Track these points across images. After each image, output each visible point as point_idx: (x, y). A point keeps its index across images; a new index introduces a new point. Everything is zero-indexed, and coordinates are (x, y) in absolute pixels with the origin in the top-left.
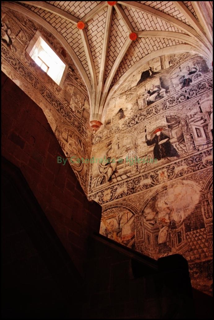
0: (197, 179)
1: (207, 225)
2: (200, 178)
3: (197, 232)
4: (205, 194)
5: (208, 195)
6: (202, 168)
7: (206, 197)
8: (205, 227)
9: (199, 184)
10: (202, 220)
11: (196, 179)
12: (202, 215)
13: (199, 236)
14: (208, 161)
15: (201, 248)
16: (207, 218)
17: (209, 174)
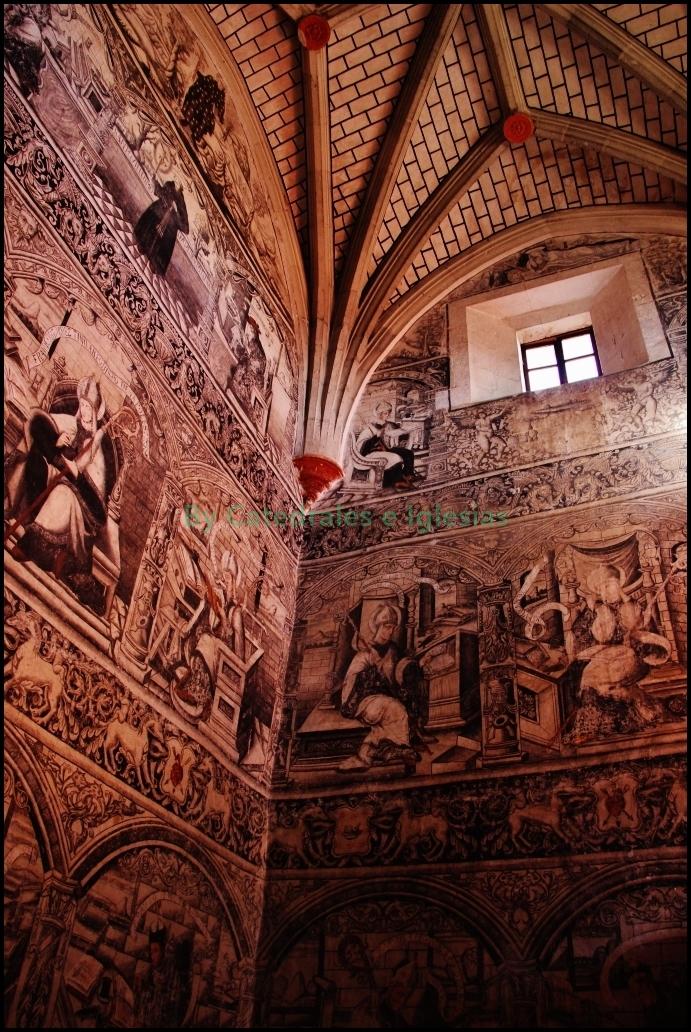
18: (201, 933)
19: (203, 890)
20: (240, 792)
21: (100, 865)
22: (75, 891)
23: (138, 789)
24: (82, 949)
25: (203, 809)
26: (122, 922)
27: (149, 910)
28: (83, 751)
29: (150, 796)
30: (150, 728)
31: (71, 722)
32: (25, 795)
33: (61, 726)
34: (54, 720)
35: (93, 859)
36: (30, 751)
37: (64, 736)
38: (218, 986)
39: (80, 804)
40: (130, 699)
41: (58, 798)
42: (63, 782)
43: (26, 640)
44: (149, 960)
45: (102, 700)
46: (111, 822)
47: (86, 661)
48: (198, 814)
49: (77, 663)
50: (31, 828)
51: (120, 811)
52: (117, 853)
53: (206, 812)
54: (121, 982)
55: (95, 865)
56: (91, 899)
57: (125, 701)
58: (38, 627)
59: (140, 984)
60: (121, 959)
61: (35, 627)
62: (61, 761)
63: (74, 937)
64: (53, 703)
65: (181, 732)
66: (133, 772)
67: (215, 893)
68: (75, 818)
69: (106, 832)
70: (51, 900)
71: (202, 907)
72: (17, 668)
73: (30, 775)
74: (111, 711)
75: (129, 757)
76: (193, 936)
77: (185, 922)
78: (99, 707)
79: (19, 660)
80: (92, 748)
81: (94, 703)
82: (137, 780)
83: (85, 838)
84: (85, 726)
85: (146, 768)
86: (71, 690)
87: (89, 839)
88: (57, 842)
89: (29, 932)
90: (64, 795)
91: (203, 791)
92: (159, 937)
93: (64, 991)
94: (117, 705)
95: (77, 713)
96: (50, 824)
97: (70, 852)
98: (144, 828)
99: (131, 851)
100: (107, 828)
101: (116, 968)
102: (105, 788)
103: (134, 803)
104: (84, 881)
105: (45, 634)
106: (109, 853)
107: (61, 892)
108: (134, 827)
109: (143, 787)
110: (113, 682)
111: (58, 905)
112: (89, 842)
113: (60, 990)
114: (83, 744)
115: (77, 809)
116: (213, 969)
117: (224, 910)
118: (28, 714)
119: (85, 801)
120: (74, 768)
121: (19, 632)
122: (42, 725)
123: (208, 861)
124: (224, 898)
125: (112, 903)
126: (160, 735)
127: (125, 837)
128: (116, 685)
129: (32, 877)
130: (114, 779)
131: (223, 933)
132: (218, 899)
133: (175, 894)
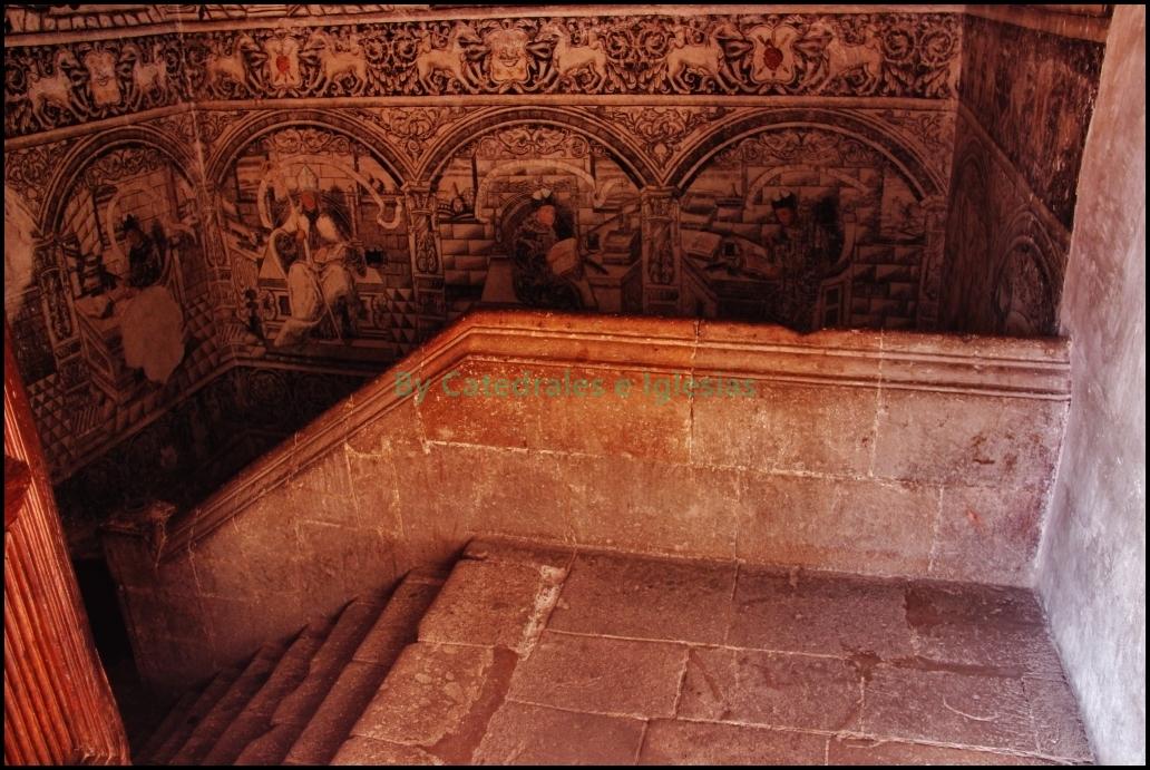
0: (19, 175)
1: (63, 361)
2: (28, 176)
3: (39, 391)
4: (48, 247)
5: (57, 254)
6: (29, 131)
7: (51, 258)
8: (55, 371)
9: (27, 199)
10: (45, 347)
11: (15, 174)
12: (45, 327)
13: (46, 400)
14: (46, 100)
15: (57, 440)
16: (60, 339)
17: (54, 165)
18: (851, 187)
19: (845, 149)
20: (904, 26)
21: (694, 168)
22: (673, 194)
23: (724, 93)
24: (696, 229)
25: (827, 73)
26: (735, 202)
27: (766, 185)
28: (646, 92)
29: (741, 92)
30: (719, 34)
31: (625, 76)
32: (602, 147)
33: (617, 84)
34: (608, 83)
35: (688, 164)
36: (593, 116)
37: (623, 90)
38: (887, 228)
39: (657, 132)
40: (683, 22)
41: (633, 138)
42: (634, 124)
43: (556, 43)
44: (778, 222)
45: (650, 42)
46: (696, 133)
47: (621, 21)
48: (820, 81)
49: (612, 28)
50: (617, 166)
51: (705, 120)
52: (713, 152)
53: (831, 76)
54: (746, 244)
55: (688, 170)
56: (691, 195)
57: (678, 28)
58: (563, 26)
59: (771, 242)
60: (738, 228)
61: (560, 28)
62: (625, 110)
63: (683, 223)
64: (601, 71)
65: (765, 17)
66: (711, 83)
67: (867, 146)
68: (655, 144)
69: (695, 142)
70: (652, 206)
71: (846, 164)
72: (558, 66)
73: (601, 133)
74: (664, 45)
75: (701, 72)
76: (838, 192)
77: (821, 183)
78: (650, 50)
79: (558, 61)
80: (658, 83)
81: (642, 49)
82: (718, 86)
83: (672, 154)
84: (640, 72)
85: (726, 71)
86: (615, 53)
87: (675, 153)
88: (644, 166)
89: (639, 229)
90: (639, 132)
91: (821, 57)
92: (789, 202)
93: (687, 258)
94: (669, 37)
95: (629, 67)
96: (632, 158)
97: (659, 169)
98: (738, 124)
99: (729, 146)
100: (696, 137)
101: (736, 235)
102: (680, 109)
103: (719, 107)
104: (680, 185)
105: (572, 27)
106: (700, 157)
107: (659, 198)
108: (726, 126)
109: (727, 89)
110: (656, 21)
111: (660, 207)
112: (676, 156)
113: (682, 257)
114: (643, 87)
115: (654, 136)
116: (877, 213)
117: (885, 158)
118: (583, 92)
119: (661, 128)
120: (642, 108)
121: (546, 42)
122: (598, 93)
123: (847, 120)
124: (885, 147)
125: (716, 191)
126: (737, 35)
127: (718, 138)
128: (661, 21)
129: (629, 196)
130: (691, 98)
131: (886, 179)
132: (874, 150)
133: (801, 163)
